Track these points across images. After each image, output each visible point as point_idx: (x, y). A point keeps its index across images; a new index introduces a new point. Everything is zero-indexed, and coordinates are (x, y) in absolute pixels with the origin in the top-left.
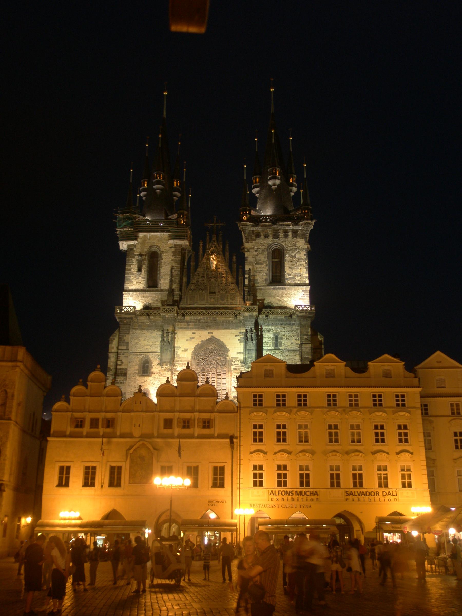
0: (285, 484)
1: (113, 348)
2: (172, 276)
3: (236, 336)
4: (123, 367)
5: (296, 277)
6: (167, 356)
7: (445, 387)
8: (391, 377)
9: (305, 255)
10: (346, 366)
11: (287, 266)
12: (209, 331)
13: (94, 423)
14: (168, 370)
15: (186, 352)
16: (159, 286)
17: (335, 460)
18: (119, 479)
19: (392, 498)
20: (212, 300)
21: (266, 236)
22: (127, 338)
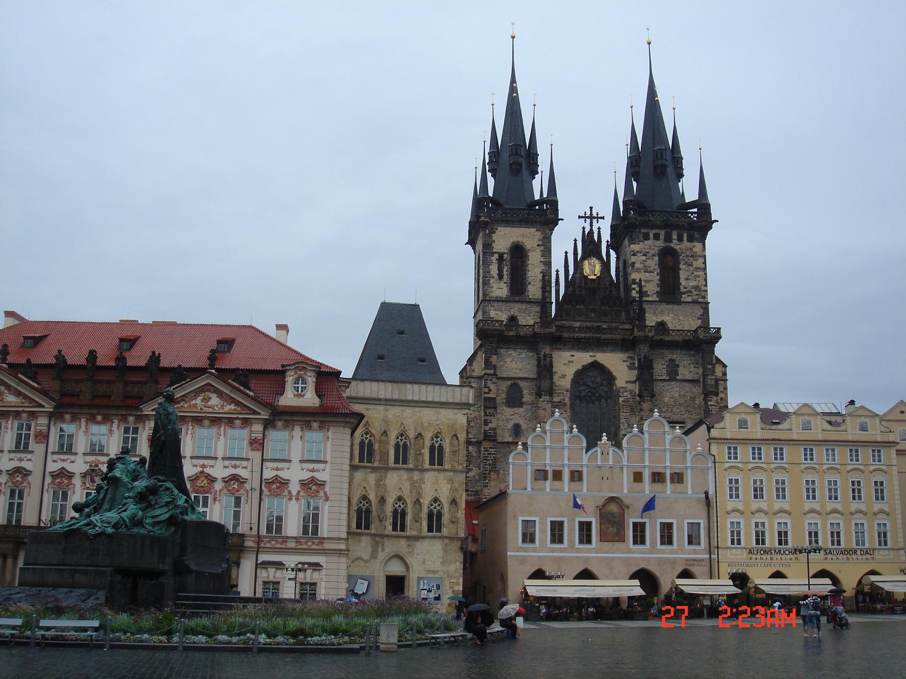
0: (763, 543)
1: (474, 371)
11: (683, 275)
13: (557, 475)
17: (812, 519)
19: (868, 556)
21: (657, 237)
22: (494, 359)
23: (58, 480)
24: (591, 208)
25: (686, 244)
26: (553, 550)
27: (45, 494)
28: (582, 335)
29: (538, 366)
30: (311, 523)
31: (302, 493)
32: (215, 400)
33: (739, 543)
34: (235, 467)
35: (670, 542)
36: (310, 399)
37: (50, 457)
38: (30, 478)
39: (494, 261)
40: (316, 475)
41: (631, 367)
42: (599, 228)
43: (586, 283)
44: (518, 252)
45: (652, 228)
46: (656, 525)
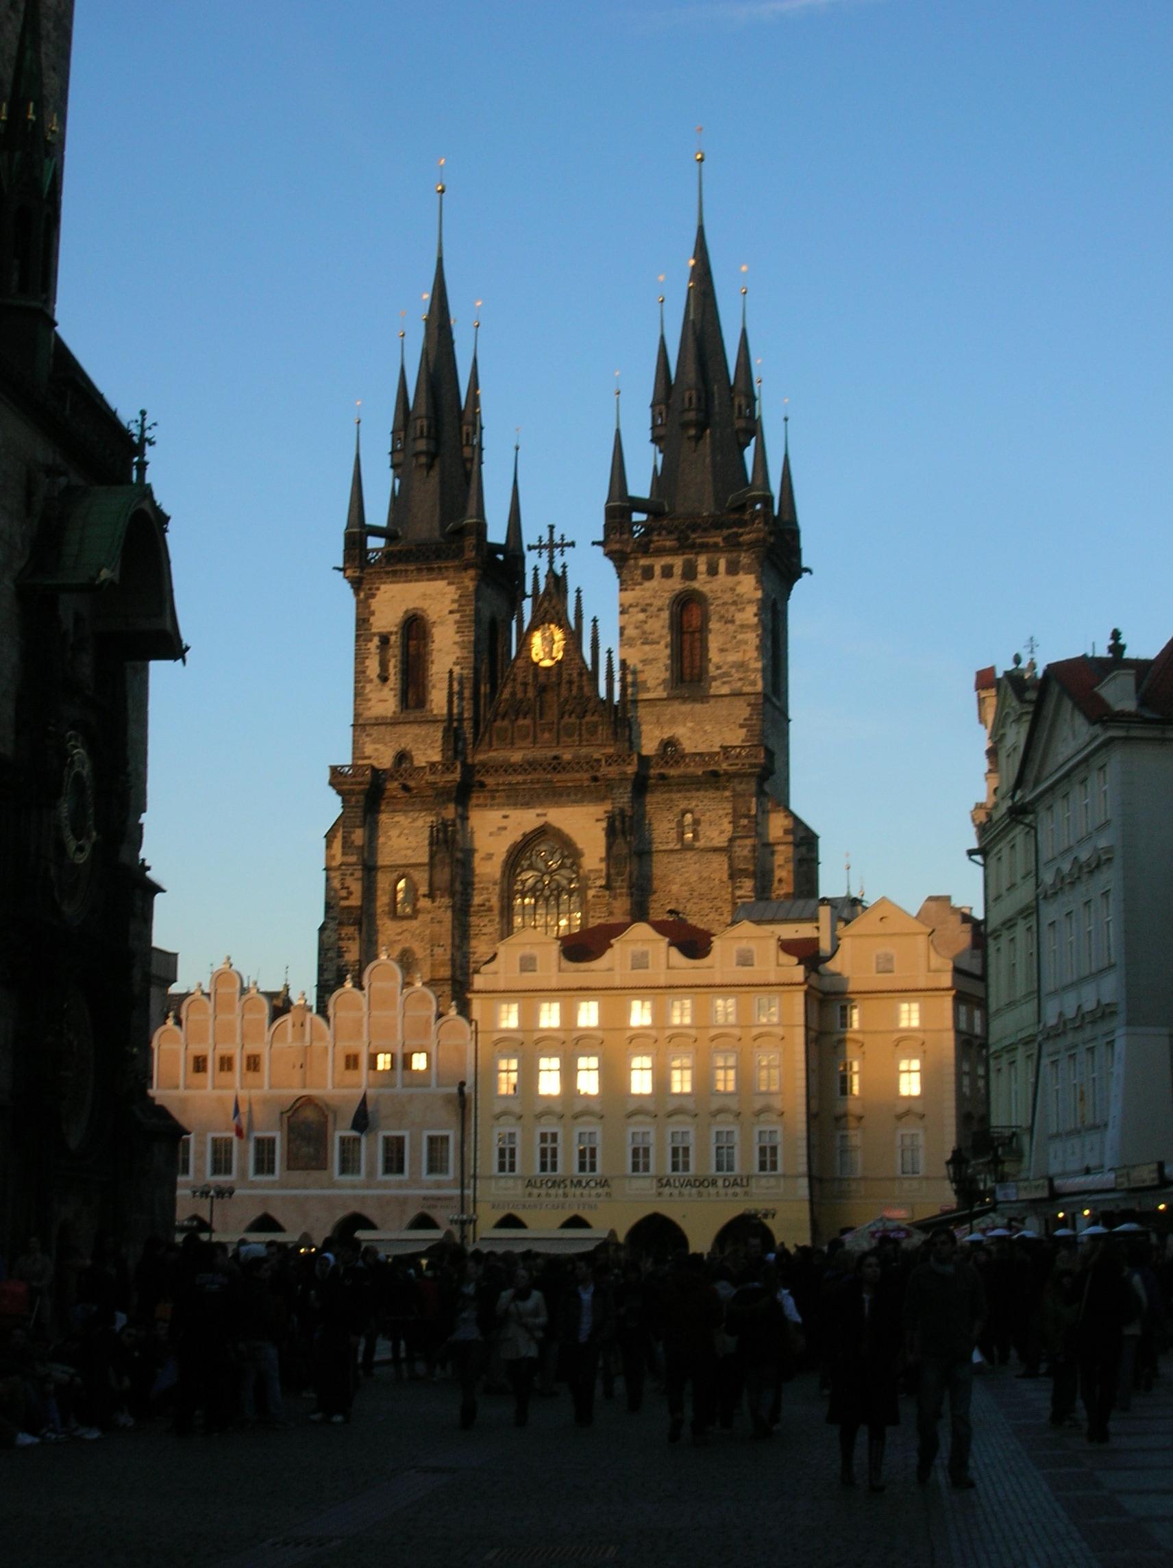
0: (554, 1168)
2: (451, 686)
3: (598, 820)
4: (355, 901)
5: (734, 670)
6: (444, 875)
7: (891, 971)
8: (752, 965)
9: (756, 615)
10: (671, 944)
11: (714, 643)
12: (539, 811)
13: (226, 1063)
14: (447, 907)
15: (489, 863)
16: (428, 707)
18: (272, 1161)
19: (738, 1190)
20: (547, 735)
21: (667, 572)
24: (552, 527)
25: (722, 578)
28: (520, 778)
29: (431, 844)
33: (512, 1169)
35: (400, 1170)
42: (564, 566)
43: (536, 676)
44: (415, 628)
45: (660, 552)
46: (376, 1141)
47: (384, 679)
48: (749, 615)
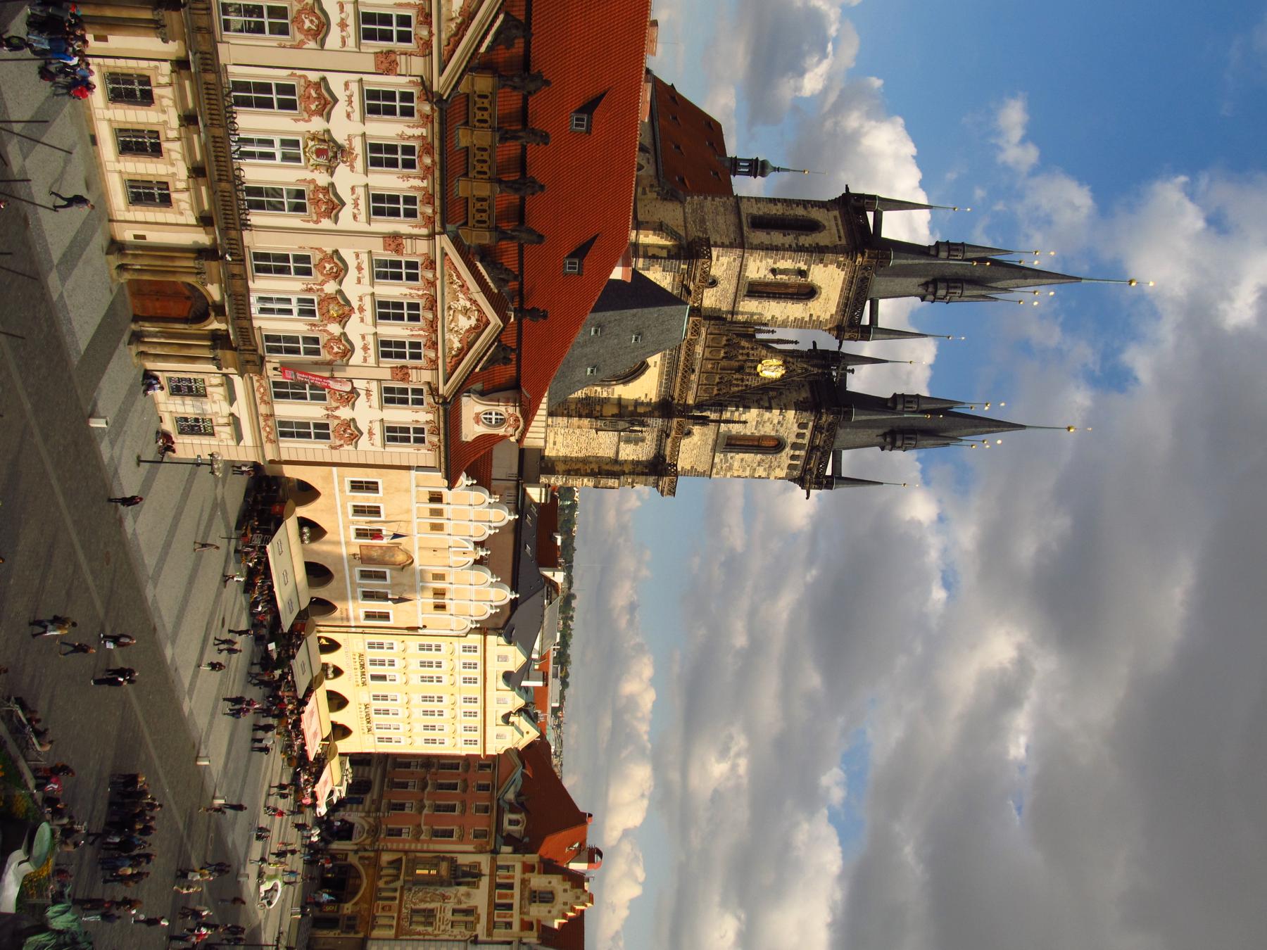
1: (647, 236)
11: (746, 456)
21: (799, 436)
23: (314, 94)
26: (344, 507)
27: (289, 72)
30: (297, 430)
31: (336, 422)
32: (465, 323)
34: (365, 348)
36: (471, 430)
37: (357, 76)
38: (312, 44)
39: (798, 265)
40: (366, 436)
41: (637, 403)
47: (774, 271)
48: (761, 472)
